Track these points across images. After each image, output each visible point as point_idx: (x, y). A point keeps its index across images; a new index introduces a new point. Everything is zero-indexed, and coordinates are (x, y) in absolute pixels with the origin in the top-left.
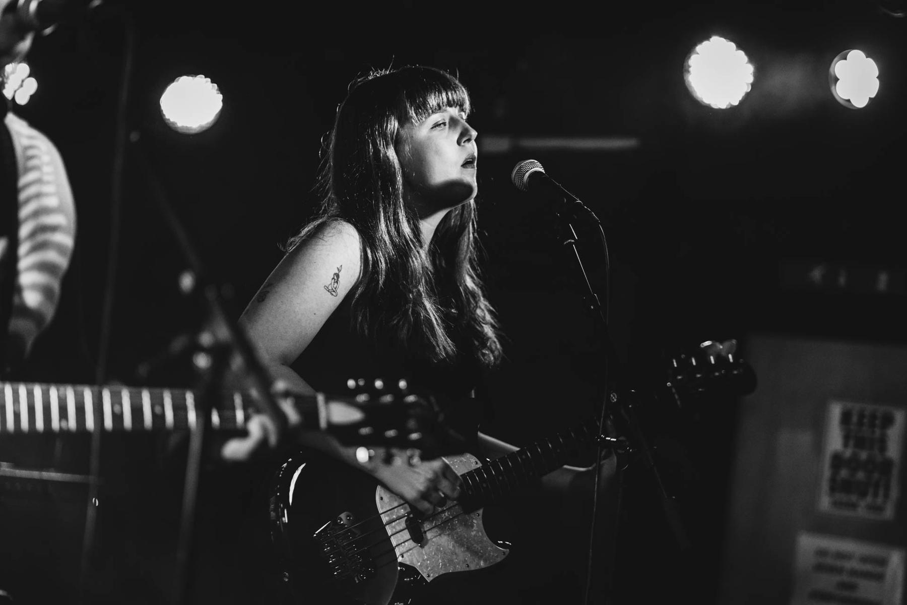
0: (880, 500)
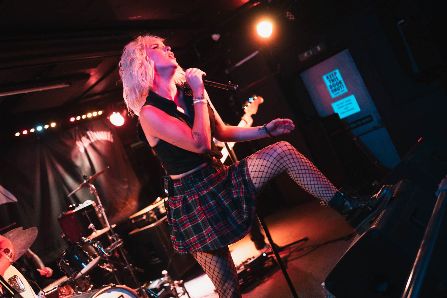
0: (343, 89)
